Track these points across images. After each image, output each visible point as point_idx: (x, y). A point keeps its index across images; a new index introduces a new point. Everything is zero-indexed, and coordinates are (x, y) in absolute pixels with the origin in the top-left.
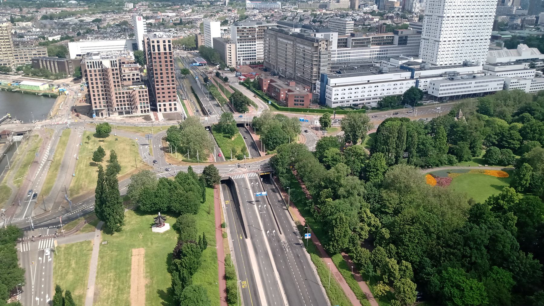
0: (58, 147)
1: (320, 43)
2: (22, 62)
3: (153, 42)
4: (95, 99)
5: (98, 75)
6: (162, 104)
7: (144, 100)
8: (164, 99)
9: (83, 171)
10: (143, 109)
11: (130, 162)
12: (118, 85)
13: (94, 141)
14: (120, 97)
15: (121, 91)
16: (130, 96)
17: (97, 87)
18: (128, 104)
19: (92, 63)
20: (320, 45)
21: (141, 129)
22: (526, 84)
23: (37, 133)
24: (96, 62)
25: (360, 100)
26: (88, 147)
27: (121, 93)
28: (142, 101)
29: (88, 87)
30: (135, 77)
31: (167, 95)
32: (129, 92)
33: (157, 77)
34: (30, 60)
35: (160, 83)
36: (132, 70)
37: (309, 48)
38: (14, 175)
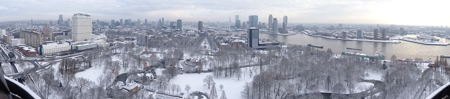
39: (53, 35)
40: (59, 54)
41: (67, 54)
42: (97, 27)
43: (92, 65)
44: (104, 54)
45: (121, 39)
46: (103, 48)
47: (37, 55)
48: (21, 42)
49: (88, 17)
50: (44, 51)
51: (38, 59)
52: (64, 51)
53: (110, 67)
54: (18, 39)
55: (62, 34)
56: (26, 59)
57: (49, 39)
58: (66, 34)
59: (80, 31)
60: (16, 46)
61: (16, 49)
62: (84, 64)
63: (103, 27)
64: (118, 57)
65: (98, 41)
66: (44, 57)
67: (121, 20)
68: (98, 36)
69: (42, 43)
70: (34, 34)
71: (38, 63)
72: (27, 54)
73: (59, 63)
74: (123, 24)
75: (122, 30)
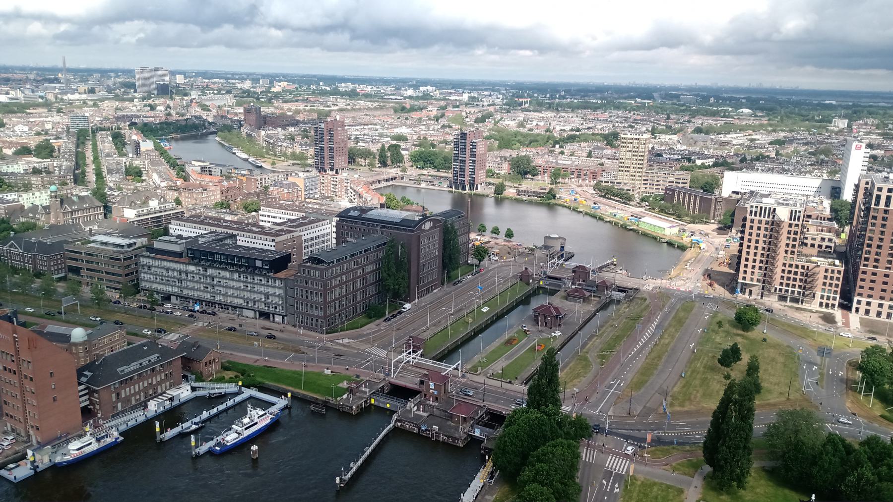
0: (670, 325)
2: (651, 191)
3: (880, 189)
4: (746, 266)
5: (763, 229)
6: (864, 300)
7: (831, 285)
8: (870, 292)
9: (698, 373)
10: (825, 301)
11: (778, 384)
12: (793, 252)
13: (728, 333)
14: (790, 272)
15: (795, 263)
16: (807, 274)
17: (756, 248)
18: (800, 287)
19: (759, 208)
21: (812, 334)
23: (645, 296)
24: (766, 208)
26: (715, 338)
27: (794, 266)
28: (827, 287)
29: (741, 245)
30: (824, 244)
31: (878, 286)
32: (808, 267)
33: (869, 252)
34: (662, 189)
35: (871, 263)
36: (822, 231)
38: (600, 346)
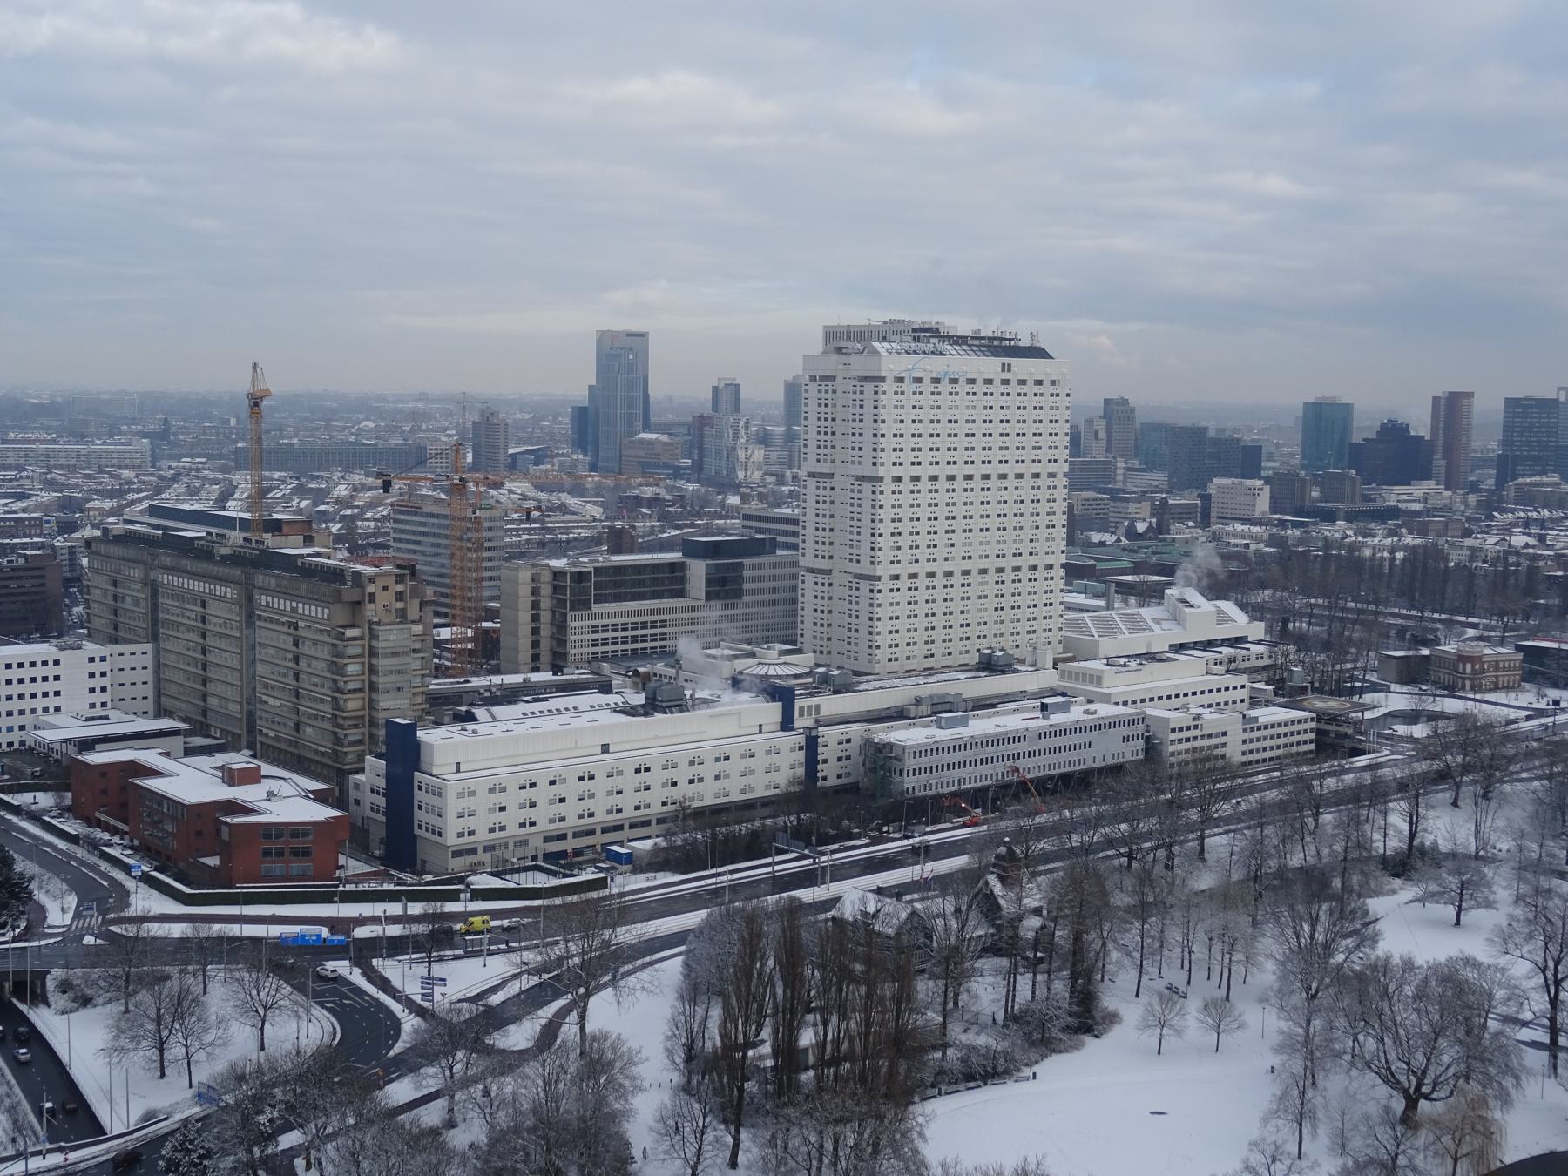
1: (371, 588)
20: (372, 596)
22: (1224, 734)
25: (576, 835)
37: (322, 613)
39: (546, 590)
40: (656, 850)
41: (754, 847)
42: (1116, 495)
43: (1109, 1000)
44: (1257, 851)
45: (1463, 658)
46: (1226, 770)
47: (355, 866)
48: (98, 698)
49: (1013, 361)
50: (453, 805)
51: (375, 920)
52: (709, 801)
53: (1371, 1044)
54: (63, 656)
55: (668, 581)
56: (216, 929)
57: (488, 651)
58: (724, 586)
59: (905, 541)
60: (29, 752)
61: (23, 799)
62: (1011, 989)
63: (1188, 498)
64: (1451, 911)
65: (1155, 679)
66: (453, 896)
67: (1452, 408)
68: (1148, 613)
69: (403, 702)
70: (304, 587)
71: (384, 984)
72: (213, 861)
73: (672, 968)
74: (1483, 462)
75: (1467, 534)
